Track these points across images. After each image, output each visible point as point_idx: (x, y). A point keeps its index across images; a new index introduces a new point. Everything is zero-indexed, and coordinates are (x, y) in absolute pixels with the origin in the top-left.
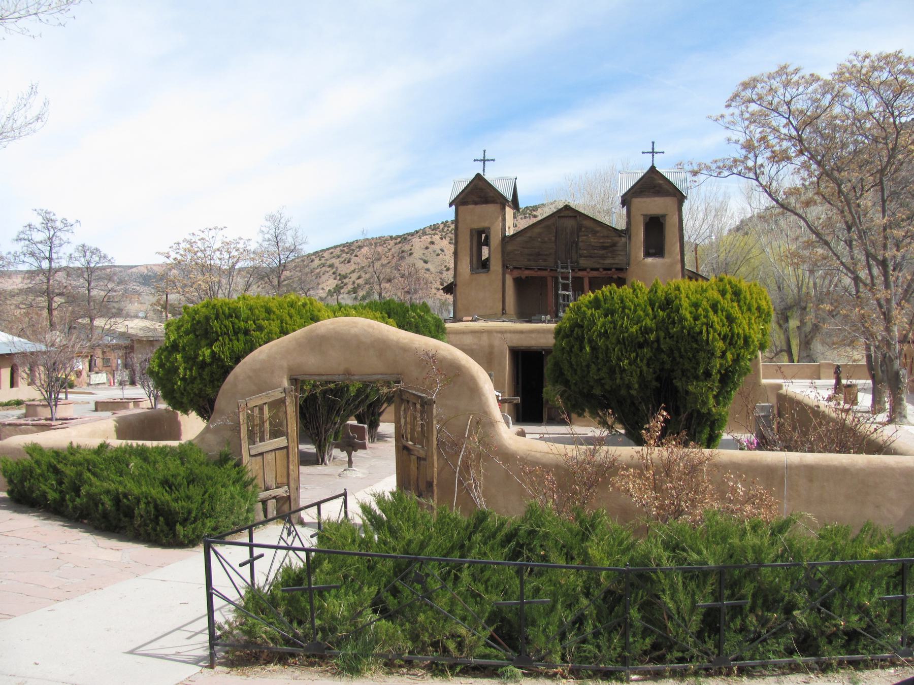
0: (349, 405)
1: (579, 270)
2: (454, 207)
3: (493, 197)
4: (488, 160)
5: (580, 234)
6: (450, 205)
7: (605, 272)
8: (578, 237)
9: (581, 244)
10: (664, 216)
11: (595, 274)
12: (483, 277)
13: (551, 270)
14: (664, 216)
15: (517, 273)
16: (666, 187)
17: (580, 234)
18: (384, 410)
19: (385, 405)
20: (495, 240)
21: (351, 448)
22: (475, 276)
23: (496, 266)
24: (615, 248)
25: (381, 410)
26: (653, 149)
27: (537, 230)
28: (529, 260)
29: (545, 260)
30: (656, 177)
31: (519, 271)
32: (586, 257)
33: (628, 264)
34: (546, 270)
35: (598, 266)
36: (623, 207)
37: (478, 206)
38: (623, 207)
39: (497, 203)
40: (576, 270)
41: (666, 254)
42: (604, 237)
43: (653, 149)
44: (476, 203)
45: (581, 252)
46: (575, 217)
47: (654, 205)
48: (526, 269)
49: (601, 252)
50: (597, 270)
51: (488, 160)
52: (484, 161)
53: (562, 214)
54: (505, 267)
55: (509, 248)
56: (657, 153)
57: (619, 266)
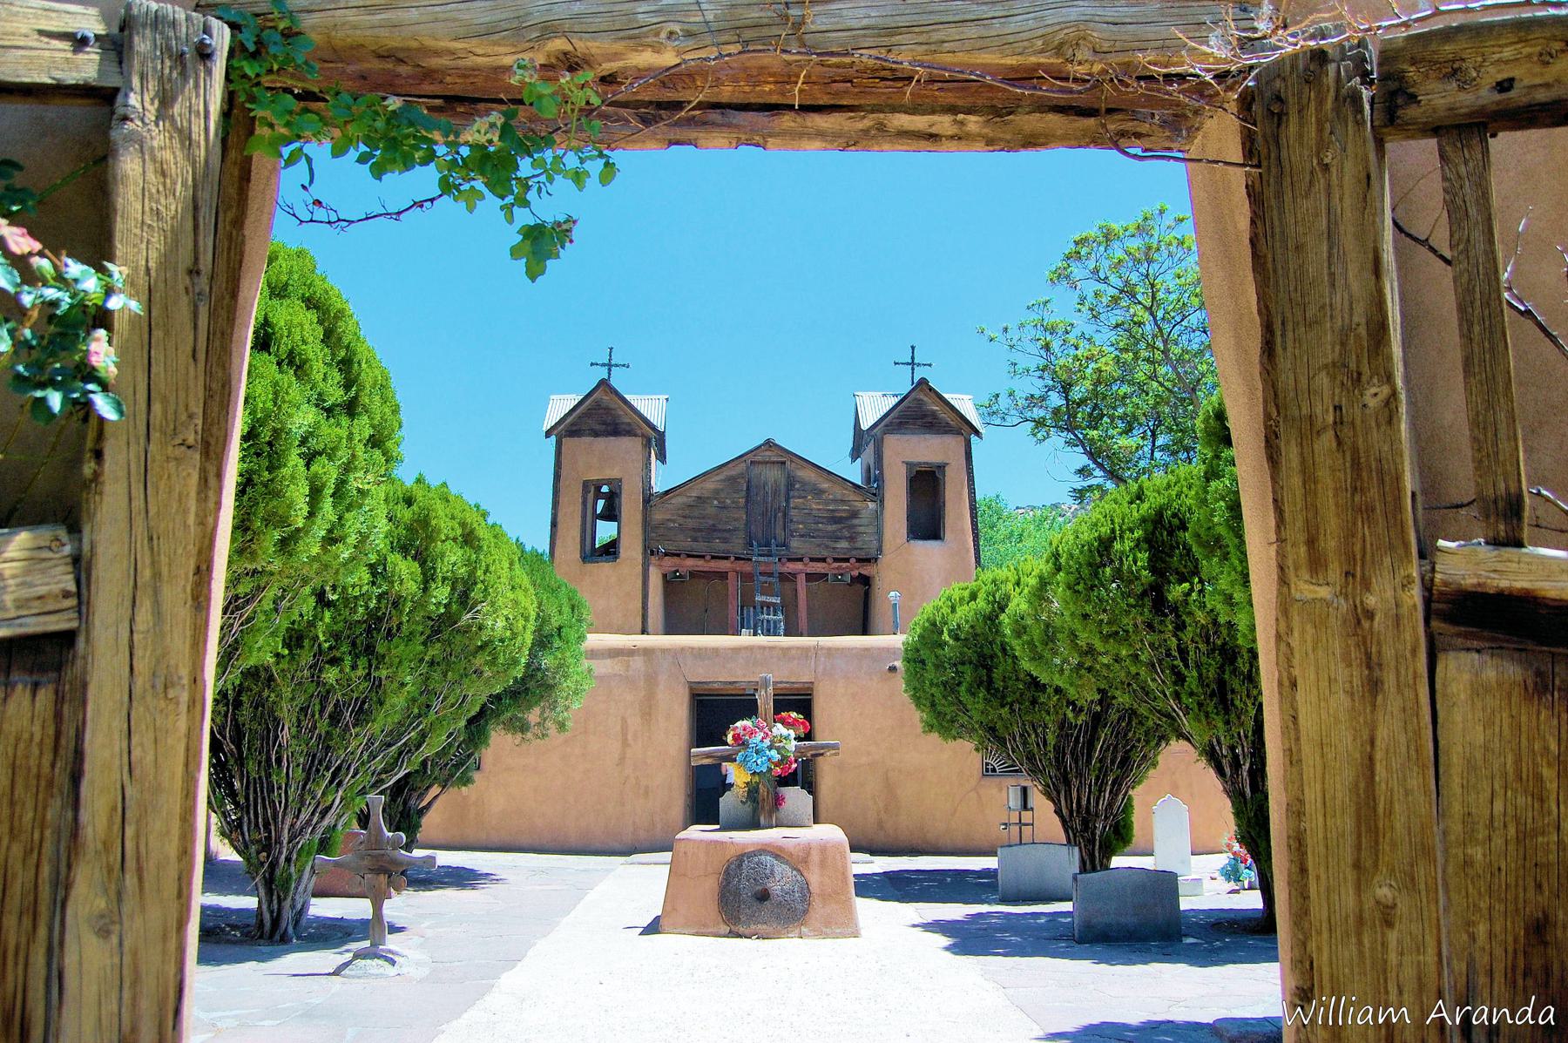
0: (373, 757)
1: (790, 560)
2: (553, 438)
3: (629, 424)
4: (617, 366)
5: (791, 493)
6: (548, 434)
7: (836, 565)
8: (787, 501)
9: (793, 512)
10: (942, 467)
11: (819, 567)
12: (604, 568)
13: (737, 559)
14: (942, 467)
15: (669, 563)
16: (945, 416)
17: (791, 493)
18: (430, 804)
19: (435, 790)
20: (630, 506)
21: (383, 878)
22: (590, 566)
23: (632, 550)
24: (856, 522)
25: (424, 804)
26: (913, 358)
27: (710, 485)
28: (695, 540)
29: (725, 540)
30: (925, 399)
31: (676, 560)
32: (802, 536)
33: (880, 549)
34: (727, 558)
35: (825, 553)
36: (854, 460)
37: (599, 439)
38: (854, 460)
39: (636, 435)
40: (784, 560)
41: (948, 535)
42: (835, 501)
43: (913, 358)
44: (596, 434)
45: (793, 527)
46: (784, 463)
47: (926, 449)
48: (689, 556)
49: (830, 528)
50: (824, 560)
51: (617, 366)
52: (610, 366)
53: (758, 458)
54: (649, 551)
55: (658, 516)
56: (919, 365)
57: (862, 555)
